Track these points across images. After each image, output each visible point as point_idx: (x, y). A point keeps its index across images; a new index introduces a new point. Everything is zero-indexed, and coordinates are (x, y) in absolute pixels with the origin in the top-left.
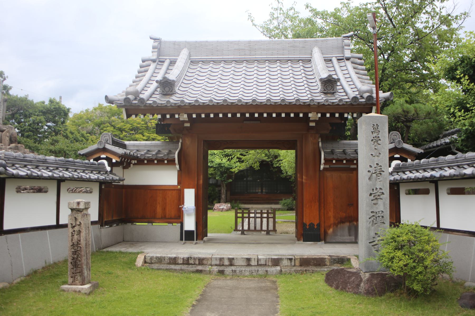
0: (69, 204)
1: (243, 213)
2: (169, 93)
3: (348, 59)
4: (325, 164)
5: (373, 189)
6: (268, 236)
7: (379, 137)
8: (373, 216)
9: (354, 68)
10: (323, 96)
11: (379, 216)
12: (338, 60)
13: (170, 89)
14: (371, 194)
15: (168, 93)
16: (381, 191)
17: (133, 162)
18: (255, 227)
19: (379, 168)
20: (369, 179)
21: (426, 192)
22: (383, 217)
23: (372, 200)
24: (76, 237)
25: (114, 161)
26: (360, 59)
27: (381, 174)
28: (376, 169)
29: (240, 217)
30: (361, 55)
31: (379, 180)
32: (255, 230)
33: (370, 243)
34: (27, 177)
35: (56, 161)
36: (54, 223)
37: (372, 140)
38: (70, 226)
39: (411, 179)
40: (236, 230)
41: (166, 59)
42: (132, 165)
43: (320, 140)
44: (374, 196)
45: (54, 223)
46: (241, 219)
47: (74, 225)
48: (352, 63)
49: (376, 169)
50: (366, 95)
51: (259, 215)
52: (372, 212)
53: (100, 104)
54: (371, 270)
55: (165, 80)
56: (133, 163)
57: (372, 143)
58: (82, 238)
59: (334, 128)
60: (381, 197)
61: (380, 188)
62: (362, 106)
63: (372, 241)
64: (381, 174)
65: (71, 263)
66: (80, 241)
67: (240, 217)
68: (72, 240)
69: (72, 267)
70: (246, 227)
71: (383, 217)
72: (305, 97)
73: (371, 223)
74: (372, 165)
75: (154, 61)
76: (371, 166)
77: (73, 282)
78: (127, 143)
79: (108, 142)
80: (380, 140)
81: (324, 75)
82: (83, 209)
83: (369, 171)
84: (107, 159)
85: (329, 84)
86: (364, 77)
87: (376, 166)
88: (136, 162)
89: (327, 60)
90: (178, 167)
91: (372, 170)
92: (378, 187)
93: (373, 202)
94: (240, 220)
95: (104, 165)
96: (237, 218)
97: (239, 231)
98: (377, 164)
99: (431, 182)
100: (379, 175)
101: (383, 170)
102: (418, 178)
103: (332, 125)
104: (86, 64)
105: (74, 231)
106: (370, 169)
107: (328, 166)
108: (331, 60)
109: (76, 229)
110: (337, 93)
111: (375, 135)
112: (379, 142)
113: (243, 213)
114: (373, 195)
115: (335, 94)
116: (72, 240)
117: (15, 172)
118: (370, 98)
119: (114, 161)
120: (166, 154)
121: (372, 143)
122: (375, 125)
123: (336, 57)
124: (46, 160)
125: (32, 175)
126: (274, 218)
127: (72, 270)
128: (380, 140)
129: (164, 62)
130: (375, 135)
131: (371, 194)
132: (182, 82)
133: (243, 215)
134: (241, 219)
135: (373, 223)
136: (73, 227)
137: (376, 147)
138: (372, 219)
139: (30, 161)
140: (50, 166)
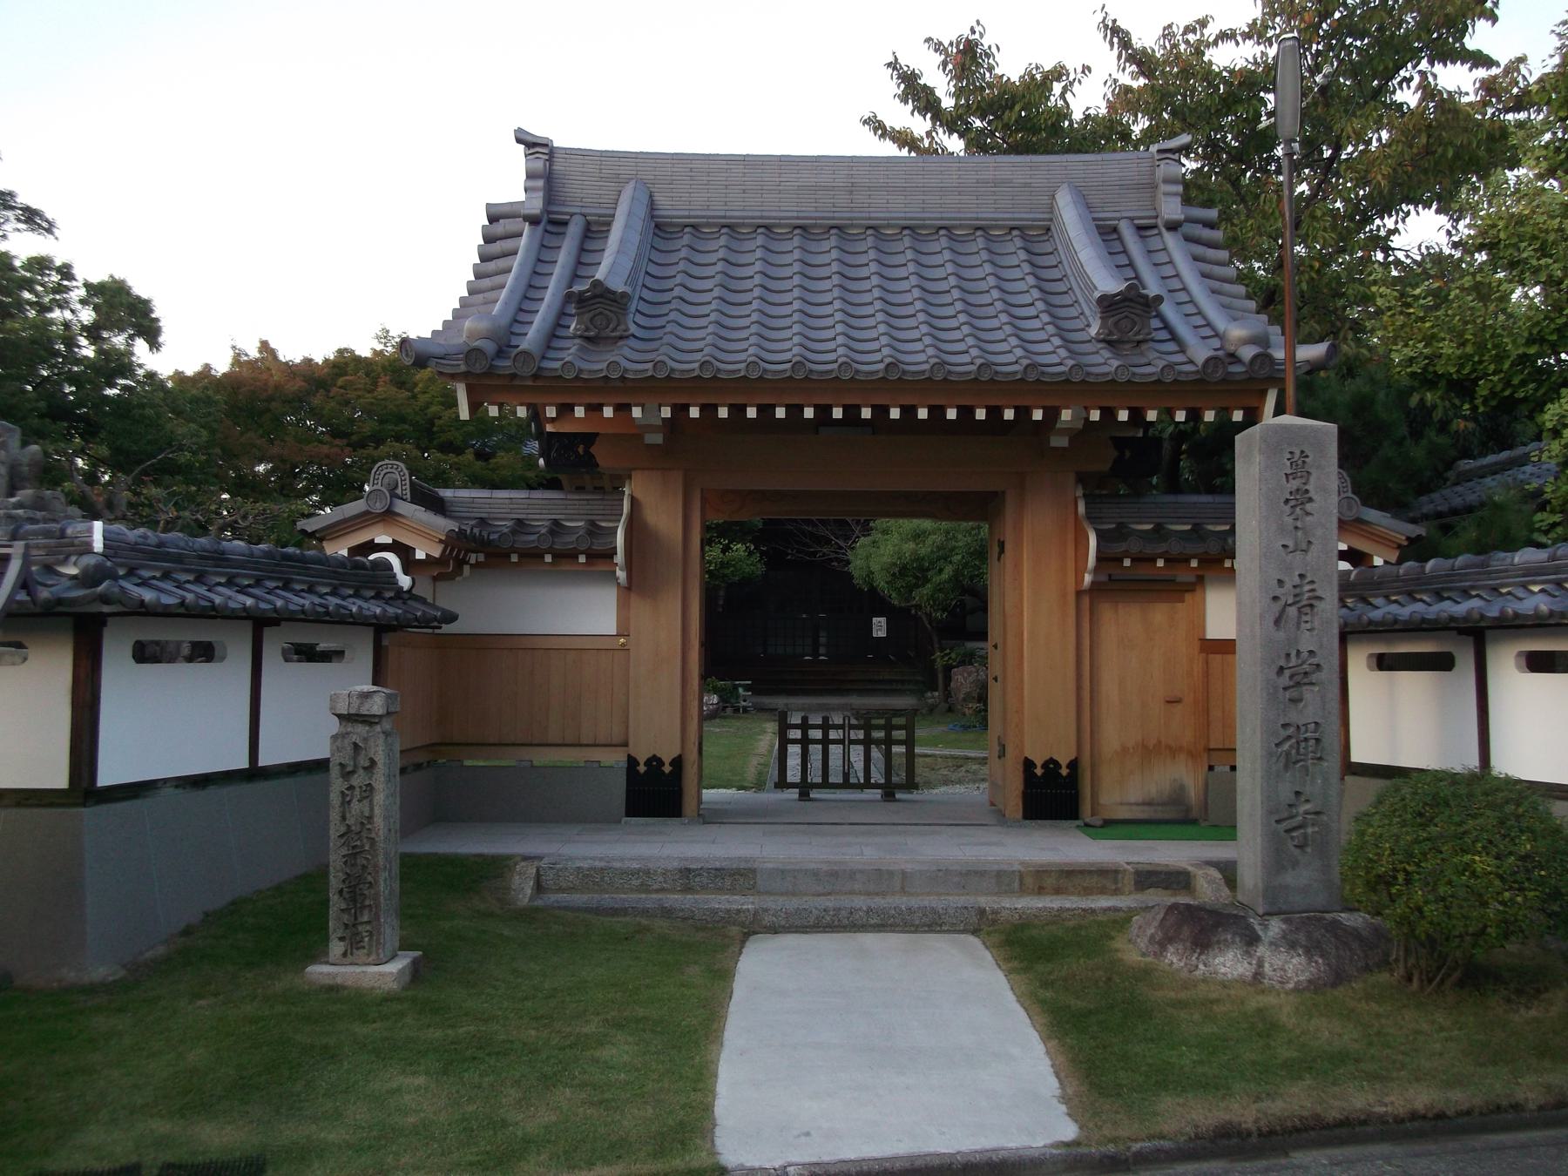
0: (334, 699)
1: (889, 728)
2: (607, 332)
3: (1173, 227)
4: (1096, 570)
5: (1288, 655)
6: (892, 806)
7: (1307, 491)
8: (1289, 737)
9: (1196, 259)
10: (1106, 354)
11: (1306, 740)
12: (1140, 228)
13: (609, 322)
14: (1281, 670)
15: (603, 334)
16: (1314, 660)
17: (473, 558)
18: (846, 776)
19: (1307, 588)
20: (1277, 622)
21: (1441, 663)
22: (1317, 740)
23: (1285, 689)
24: (356, 806)
25: (420, 555)
26: (1211, 225)
27: (1311, 606)
28: (1298, 591)
29: (794, 742)
30: (1213, 214)
31: (1308, 626)
32: (846, 784)
33: (1278, 822)
34: (182, 610)
35: (252, 555)
36: (244, 763)
37: (1287, 501)
38: (335, 771)
39: (1396, 621)
40: (782, 784)
41: (572, 215)
42: (466, 569)
43: (1080, 492)
44: (1291, 677)
45: (244, 763)
46: (861, 748)
47: (349, 769)
48: (1188, 239)
49: (1298, 591)
50: (1247, 353)
51: (900, 734)
52: (1285, 726)
53: (264, 345)
54: (1284, 907)
55: (598, 291)
56: (473, 561)
57: (1287, 509)
58: (377, 811)
59: (1128, 454)
60: (1314, 678)
61: (1311, 652)
62: (1240, 386)
63: (1286, 815)
64: (1311, 606)
65: (341, 892)
66: (370, 818)
67: (794, 742)
68: (344, 818)
69: (343, 906)
70: (815, 776)
71: (1317, 740)
72: (1055, 358)
73: (1283, 760)
74: (1286, 579)
75: (533, 221)
76: (1280, 582)
77: (345, 955)
78: (447, 493)
79: (399, 491)
80: (1310, 500)
81: (1108, 283)
82: (380, 717)
83: (1275, 598)
84: (396, 547)
85: (1129, 312)
86: (1227, 287)
87: (1297, 580)
88: (481, 558)
89: (1107, 233)
90: (621, 575)
91: (1286, 594)
92: (1304, 648)
93: (1288, 694)
94: (794, 750)
95: (389, 567)
96: (784, 742)
97: (793, 786)
98: (1302, 576)
99: (1462, 631)
100: (1307, 610)
101: (1318, 593)
102: (1424, 620)
103: (1120, 443)
104: (292, 227)
105: (351, 788)
106: (1279, 592)
107: (1104, 578)
108: (1115, 230)
109: (358, 780)
110: (1151, 344)
111: (1294, 484)
112: (1308, 507)
113: (889, 728)
114: (1287, 673)
115: (1144, 347)
116: (344, 818)
117: (148, 595)
118: (1264, 358)
119: (420, 555)
120: (544, 531)
121: (1287, 509)
122: (1298, 453)
123: (1132, 219)
124: (223, 553)
125: (226, 607)
126: (910, 743)
127: (345, 918)
128: (1310, 500)
129: (565, 224)
130: (1294, 484)
131: (1281, 670)
132: (641, 298)
133: (826, 735)
134: (861, 748)
135: (1289, 762)
136: (347, 774)
137: (1299, 524)
138: (1286, 746)
139: (178, 559)
140: (238, 575)
